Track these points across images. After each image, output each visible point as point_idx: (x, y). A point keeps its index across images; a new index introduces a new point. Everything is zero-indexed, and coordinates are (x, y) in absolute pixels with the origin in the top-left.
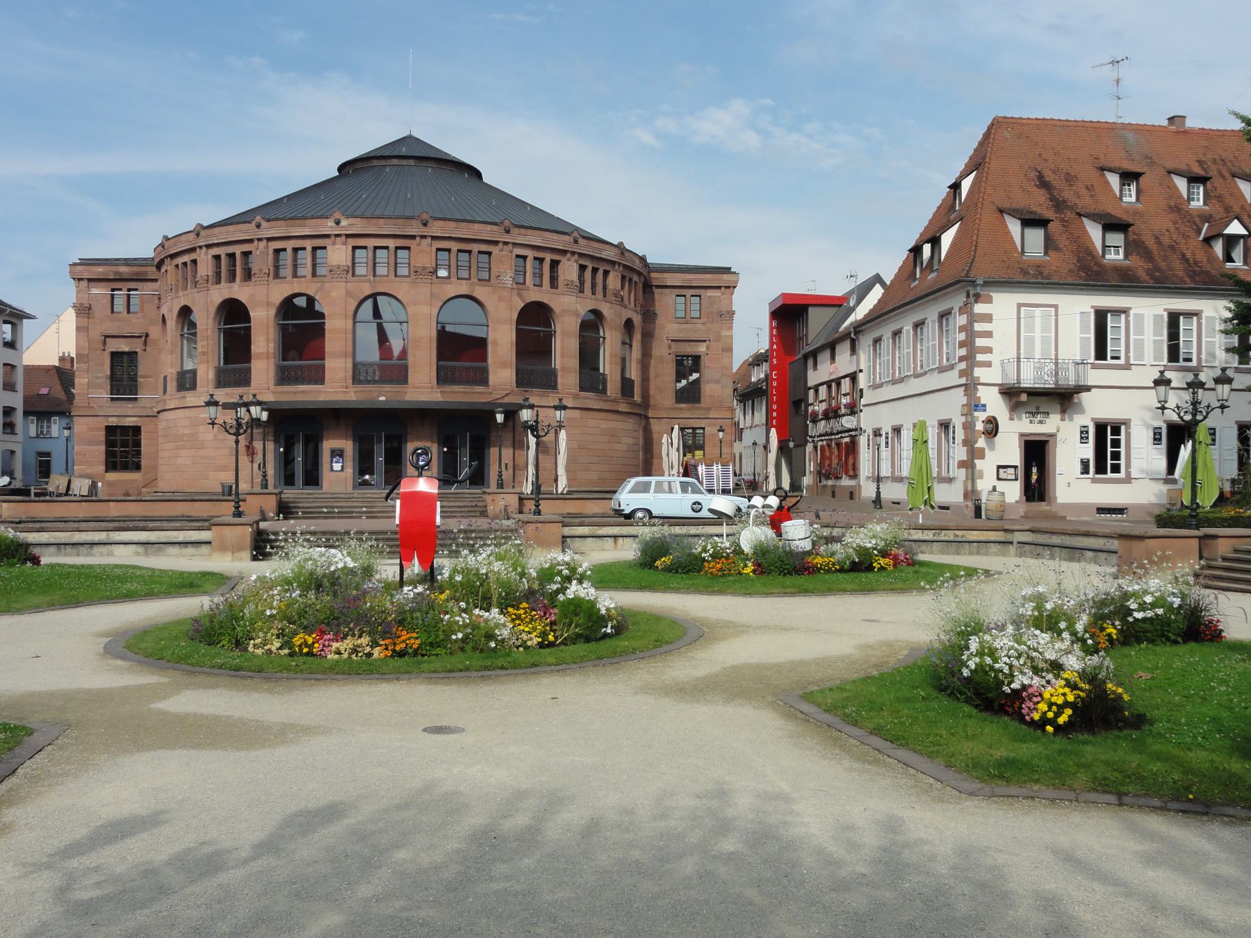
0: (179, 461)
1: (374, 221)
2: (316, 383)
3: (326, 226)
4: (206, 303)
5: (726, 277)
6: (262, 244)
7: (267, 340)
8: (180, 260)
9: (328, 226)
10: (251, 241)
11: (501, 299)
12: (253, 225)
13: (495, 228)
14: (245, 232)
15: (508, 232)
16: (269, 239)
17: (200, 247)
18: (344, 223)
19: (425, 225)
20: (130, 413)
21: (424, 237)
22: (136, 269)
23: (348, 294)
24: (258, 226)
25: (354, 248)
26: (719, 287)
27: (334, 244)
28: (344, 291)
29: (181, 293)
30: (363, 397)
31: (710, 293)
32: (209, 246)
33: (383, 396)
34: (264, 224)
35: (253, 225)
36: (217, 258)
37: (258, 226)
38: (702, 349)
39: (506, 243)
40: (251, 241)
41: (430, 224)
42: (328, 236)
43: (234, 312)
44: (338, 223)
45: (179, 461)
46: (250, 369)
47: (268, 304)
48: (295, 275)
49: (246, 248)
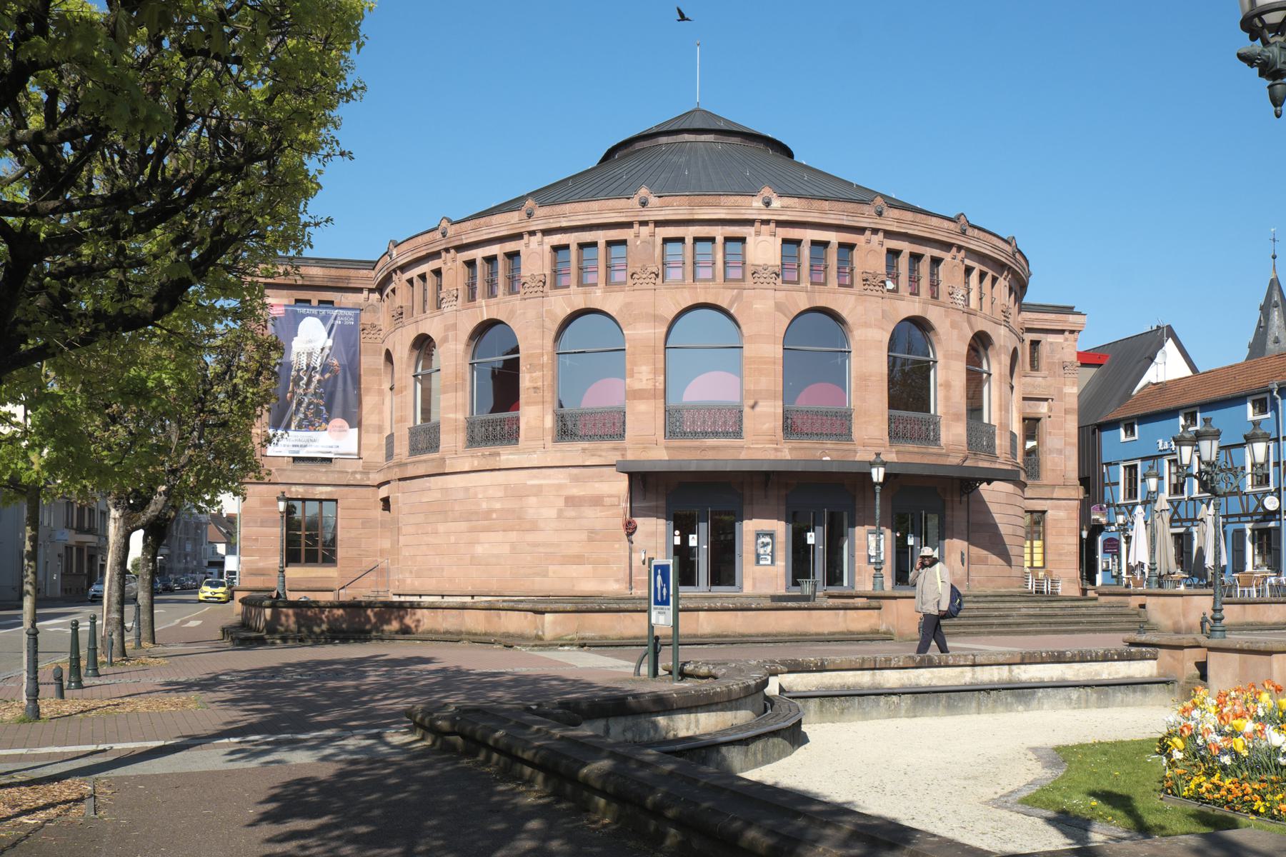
0: (479, 549)
1: (816, 204)
2: (726, 434)
3: (750, 207)
4: (452, 326)
5: (1071, 318)
6: (645, 231)
7: (655, 372)
8: (478, 254)
9: (753, 207)
10: (629, 225)
11: (954, 325)
12: (635, 202)
13: (952, 225)
14: (620, 211)
15: (964, 233)
16: (658, 223)
17: (532, 233)
18: (776, 203)
19: (880, 214)
20: (323, 480)
21: (875, 231)
22: (333, 272)
23: (779, 307)
24: (644, 204)
25: (785, 241)
26: (1062, 332)
27: (758, 233)
28: (772, 303)
29: (481, 301)
30: (836, 456)
31: (1051, 338)
32: (547, 232)
33: (823, 454)
34: (653, 200)
35: (635, 202)
36: (471, 264)
37: (644, 204)
38: (1043, 408)
39: (960, 248)
40: (629, 225)
41: (885, 214)
42: (750, 222)
43: (423, 344)
44: (767, 204)
45: (479, 549)
46: (518, 419)
47: (656, 318)
48: (608, 281)
49: (511, 246)
